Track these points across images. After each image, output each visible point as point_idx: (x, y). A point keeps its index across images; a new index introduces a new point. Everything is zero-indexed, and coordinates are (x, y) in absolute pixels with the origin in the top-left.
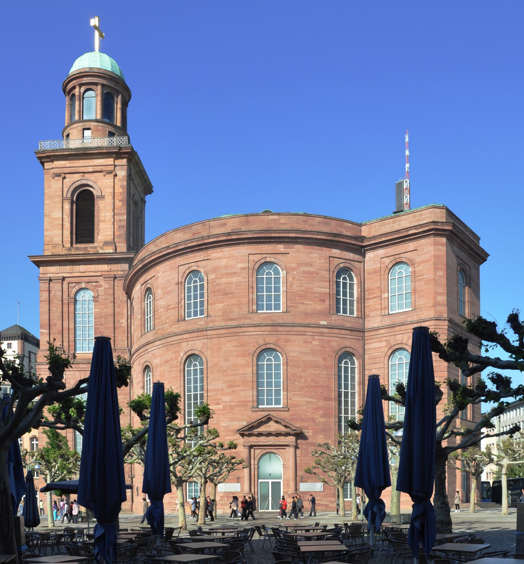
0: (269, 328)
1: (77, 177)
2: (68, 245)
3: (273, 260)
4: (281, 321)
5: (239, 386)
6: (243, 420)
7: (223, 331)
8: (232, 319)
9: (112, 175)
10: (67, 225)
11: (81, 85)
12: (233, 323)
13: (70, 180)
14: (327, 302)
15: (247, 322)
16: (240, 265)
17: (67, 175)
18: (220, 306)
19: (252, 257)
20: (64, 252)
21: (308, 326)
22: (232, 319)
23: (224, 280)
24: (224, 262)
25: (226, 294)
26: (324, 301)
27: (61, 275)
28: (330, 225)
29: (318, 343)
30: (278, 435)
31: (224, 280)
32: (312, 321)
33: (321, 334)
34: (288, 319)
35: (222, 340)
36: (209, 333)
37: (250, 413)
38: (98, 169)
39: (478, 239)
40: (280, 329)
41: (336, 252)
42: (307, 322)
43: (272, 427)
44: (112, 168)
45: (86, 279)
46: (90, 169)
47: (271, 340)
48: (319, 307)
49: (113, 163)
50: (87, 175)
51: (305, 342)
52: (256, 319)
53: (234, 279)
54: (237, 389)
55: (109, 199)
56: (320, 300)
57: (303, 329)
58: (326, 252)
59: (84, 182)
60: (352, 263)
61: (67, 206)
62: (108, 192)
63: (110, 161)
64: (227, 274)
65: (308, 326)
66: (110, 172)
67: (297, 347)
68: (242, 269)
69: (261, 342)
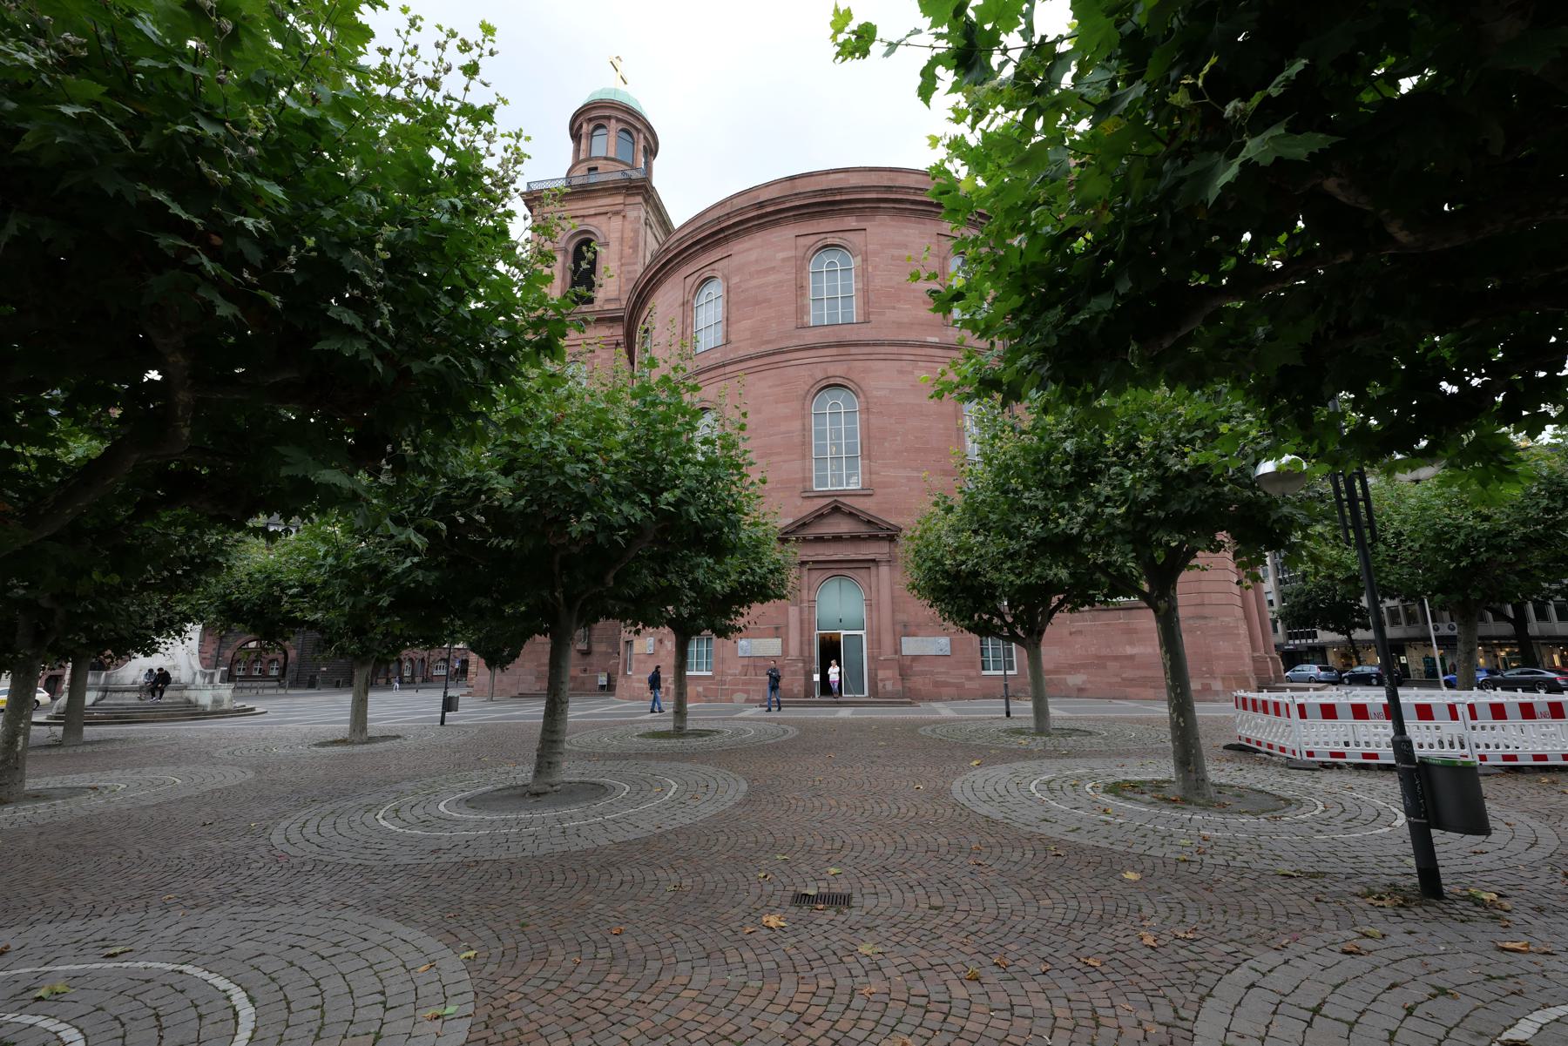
3: (837, 241)
5: (779, 454)
6: (786, 516)
8: (768, 342)
9: (620, 218)
11: (590, 120)
16: (781, 255)
18: (747, 323)
19: (802, 241)
21: (905, 344)
22: (768, 342)
23: (755, 282)
24: (753, 256)
25: (757, 303)
30: (855, 539)
31: (755, 282)
32: (912, 336)
33: (931, 359)
34: (866, 333)
36: (728, 369)
37: (799, 502)
40: (853, 350)
42: (901, 338)
43: (843, 526)
46: (592, 211)
47: (837, 370)
50: (587, 220)
51: (901, 372)
53: (772, 278)
54: (775, 459)
55: (614, 246)
57: (895, 350)
63: (619, 199)
64: (758, 272)
65: (905, 344)
66: (617, 213)
67: (884, 379)
69: (820, 375)
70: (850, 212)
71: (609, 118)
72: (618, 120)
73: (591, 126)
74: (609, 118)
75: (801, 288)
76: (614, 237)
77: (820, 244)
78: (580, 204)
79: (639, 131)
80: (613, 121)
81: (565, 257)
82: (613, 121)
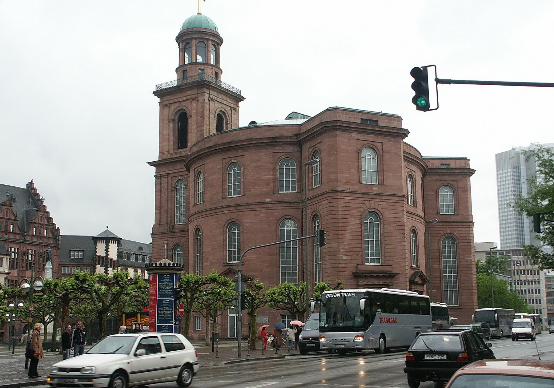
0: (232, 209)
1: (177, 105)
2: (172, 152)
3: (235, 161)
4: (239, 202)
7: (210, 212)
8: (214, 203)
10: (172, 138)
12: (214, 206)
13: (172, 108)
14: (271, 185)
15: (221, 204)
17: (171, 105)
19: (224, 161)
20: (169, 157)
21: (257, 204)
22: (214, 203)
23: (211, 178)
26: (269, 184)
27: (167, 172)
28: (273, 130)
29: (264, 215)
33: (267, 209)
34: (244, 200)
35: (209, 217)
36: (204, 213)
38: (188, 98)
39: (399, 119)
41: (278, 149)
42: (256, 201)
44: (196, 96)
45: (180, 174)
46: (184, 99)
48: (265, 189)
49: (196, 92)
50: (182, 103)
52: (225, 203)
53: (215, 176)
56: (266, 185)
58: (271, 151)
59: (181, 108)
60: (292, 154)
61: (171, 125)
62: (194, 111)
66: (194, 99)
68: (219, 169)
69: (229, 218)
70: (239, 149)
71: (191, 39)
72: (196, 39)
73: (184, 44)
74: (191, 39)
75: (223, 181)
76: (194, 111)
77: (230, 162)
78: (178, 95)
79: (208, 40)
80: (194, 40)
81: (174, 124)
82: (194, 40)
